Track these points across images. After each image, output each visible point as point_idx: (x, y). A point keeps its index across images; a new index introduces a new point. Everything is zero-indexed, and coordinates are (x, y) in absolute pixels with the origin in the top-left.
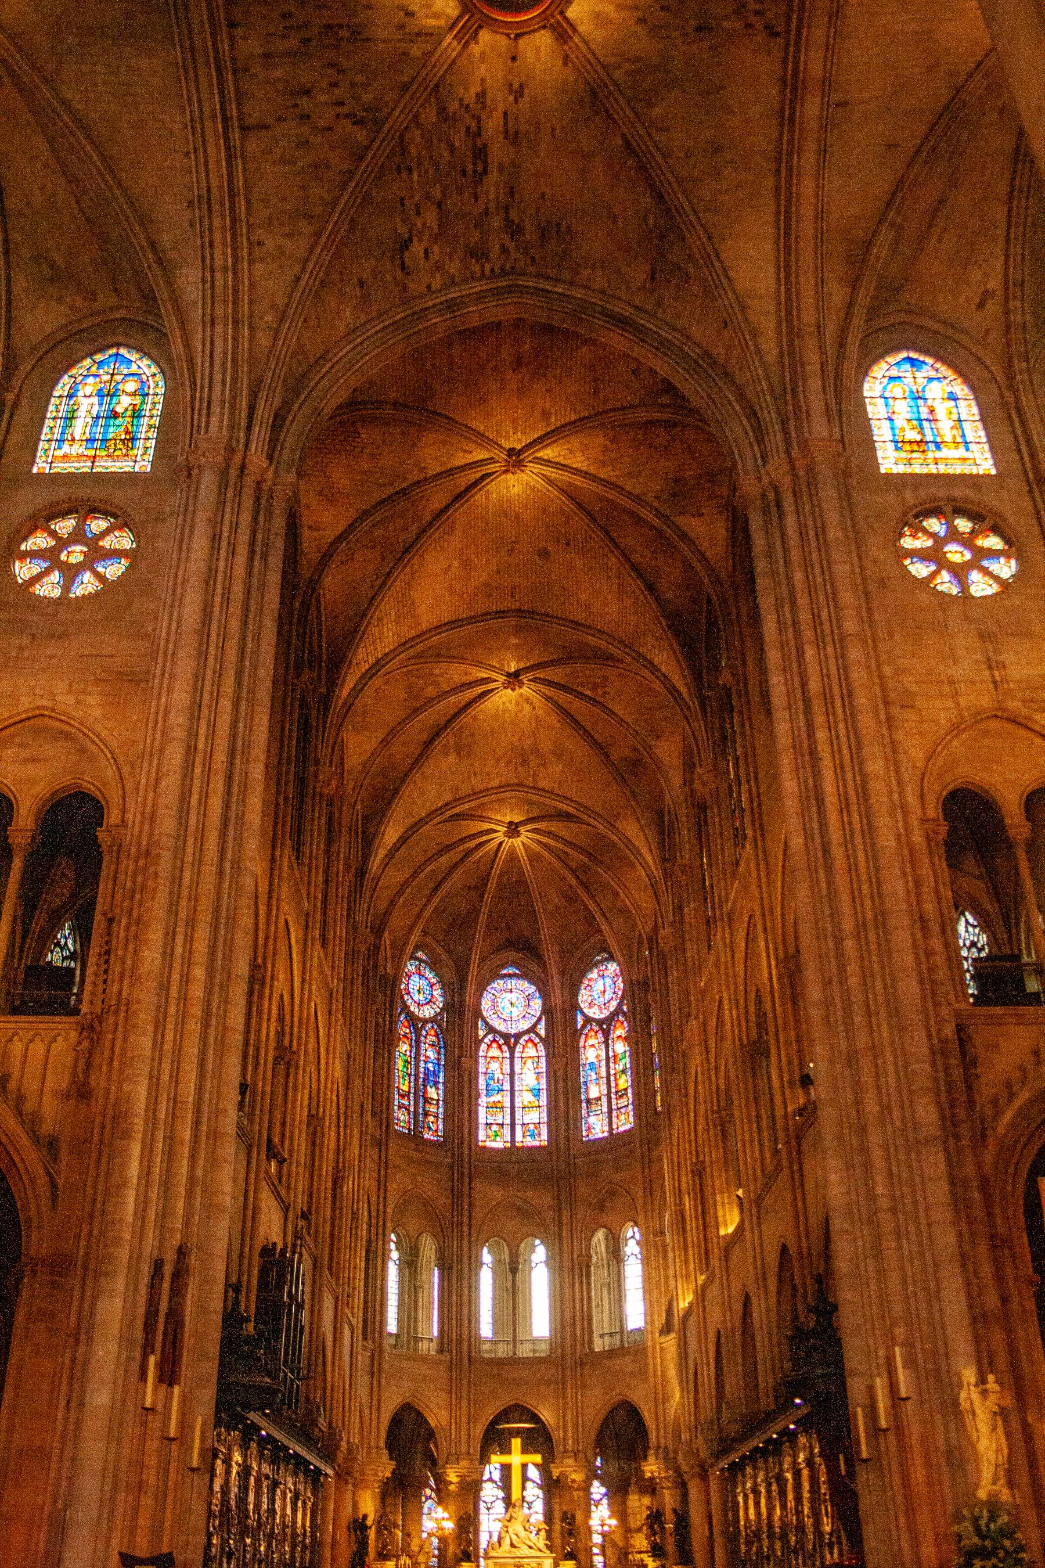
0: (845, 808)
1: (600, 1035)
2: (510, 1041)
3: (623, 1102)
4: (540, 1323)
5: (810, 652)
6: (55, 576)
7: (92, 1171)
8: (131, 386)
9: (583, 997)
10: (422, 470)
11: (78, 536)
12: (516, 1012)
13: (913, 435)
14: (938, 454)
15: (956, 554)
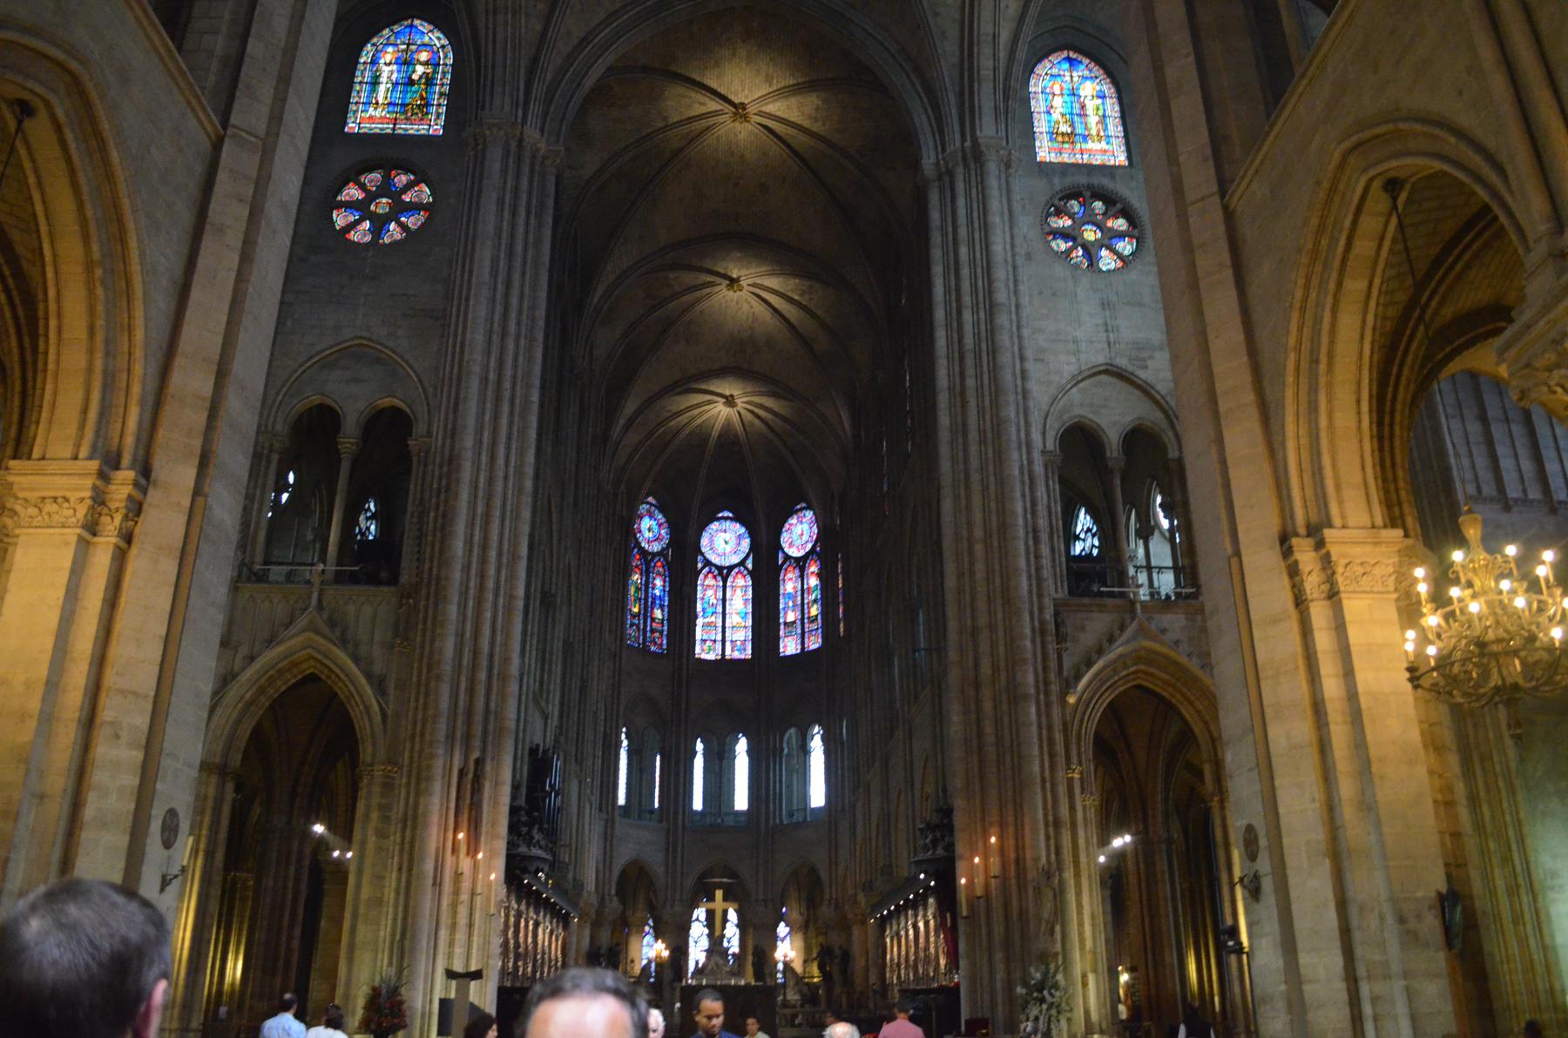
0: (983, 441)
1: (797, 572)
2: (724, 573)
3: (814, 626)
4: (741, 802)
5: (967, 316)
6: (367, 225)
7: (412, 705)
8: (424, 56)
9: (785, 539)
10: (665, 118)
11: (385, 189)
12: (728, 549)
13: (1064, 128)
14: (1084, 146)
15: (1090, 234)
